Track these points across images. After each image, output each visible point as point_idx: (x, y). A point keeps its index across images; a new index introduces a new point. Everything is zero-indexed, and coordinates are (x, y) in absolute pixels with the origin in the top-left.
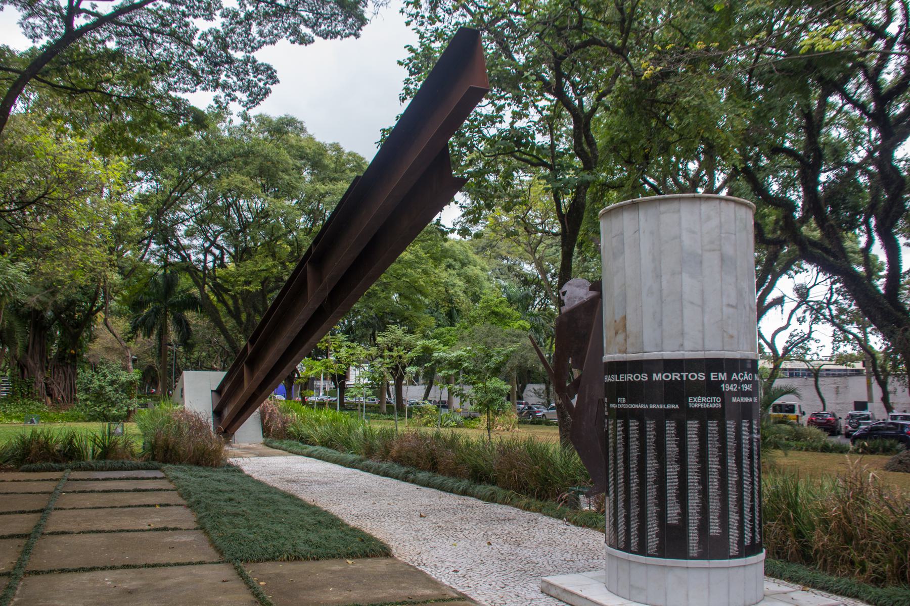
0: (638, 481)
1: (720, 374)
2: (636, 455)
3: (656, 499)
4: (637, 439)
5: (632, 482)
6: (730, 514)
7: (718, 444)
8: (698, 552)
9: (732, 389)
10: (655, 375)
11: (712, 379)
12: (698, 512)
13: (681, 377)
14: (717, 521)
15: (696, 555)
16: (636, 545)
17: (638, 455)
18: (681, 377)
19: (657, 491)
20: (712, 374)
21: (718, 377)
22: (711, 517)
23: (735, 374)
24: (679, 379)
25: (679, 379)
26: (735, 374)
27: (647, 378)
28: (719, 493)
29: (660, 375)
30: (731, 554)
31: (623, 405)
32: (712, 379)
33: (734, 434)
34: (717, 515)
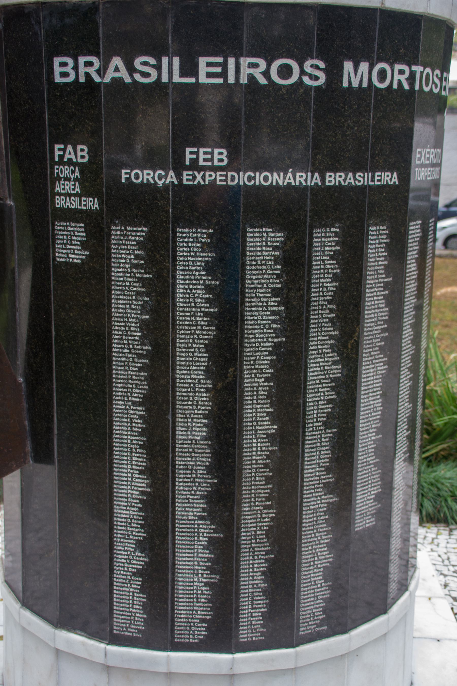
0: (272, 429)
2: (268, 346)
3: (328, 470)
4: (275, 292)
5: (248, 435)
10: (348, 66)
13: (412, 77)
16: (258, 621)
17: (277, 346)
18: (412, 77)
19: (333, 448)
24: (406, 87)
25: (406, 87)
27: (322, 78)
29: (364, 67)
31: (209, 176)
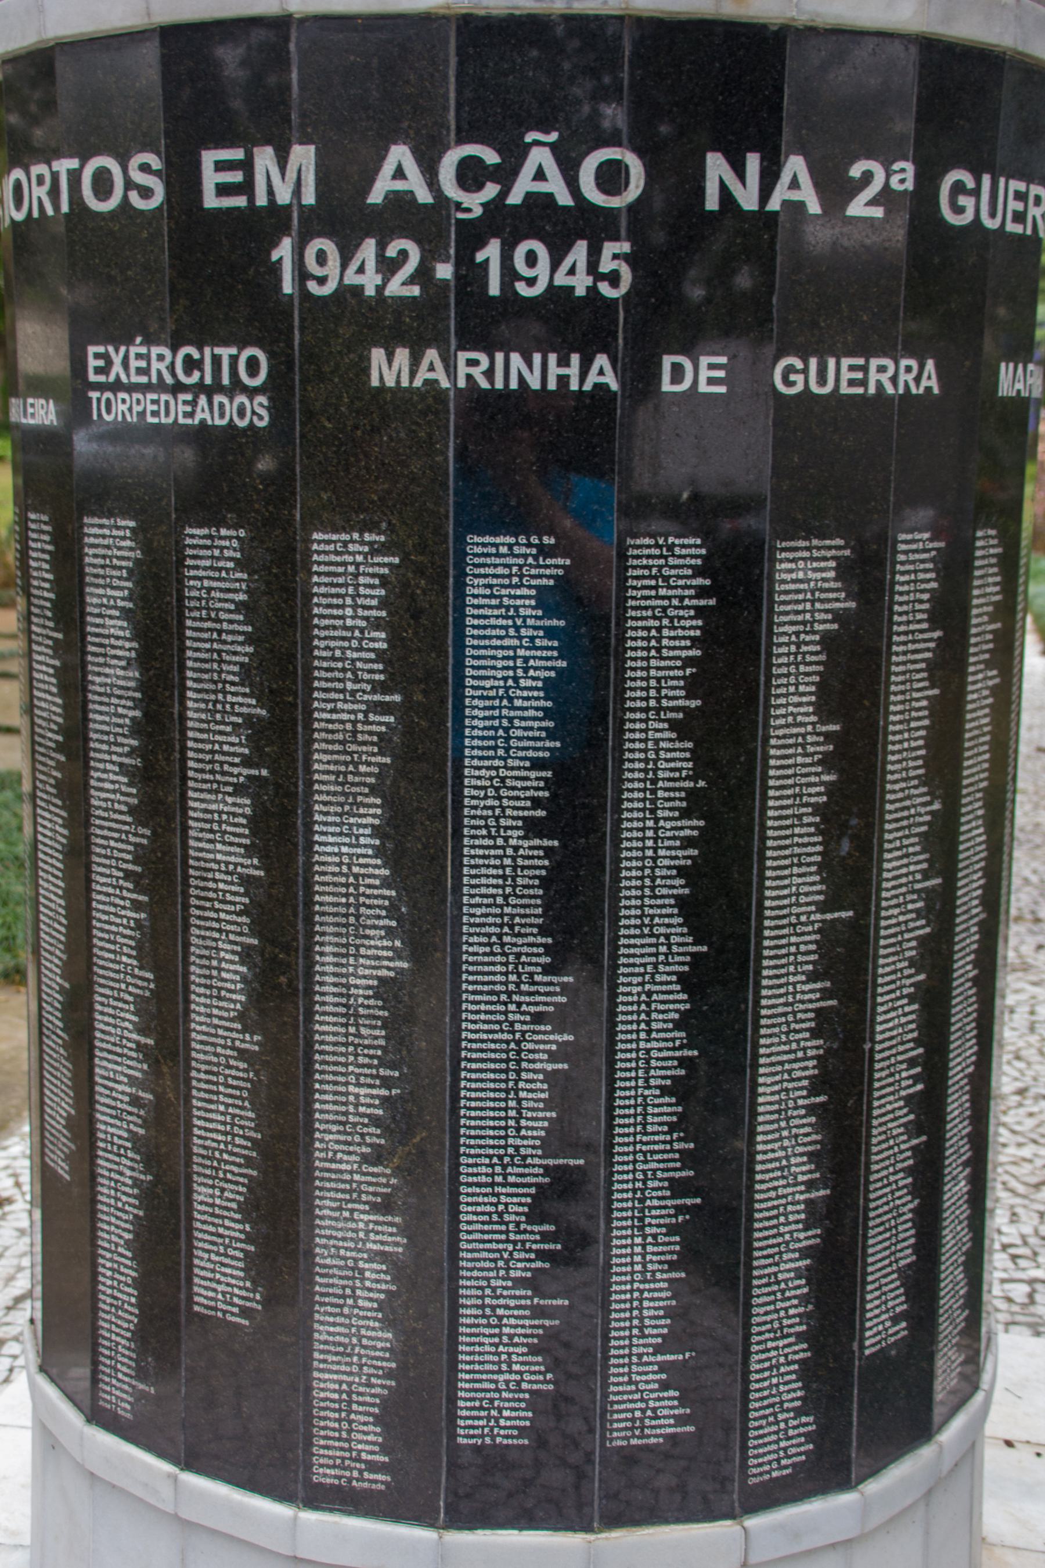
1: (265, 158)
6: (325, 1205)
7: (245, 704)
8: (140, 1396)
9: (370, 282)
11: (211, 201)
12: (133, 1137)
14: (235, 1228)
15: (125, 1410)
20: (209, 158)
21: (247, 188)
22: (202, 1193)
23: (400, 154)
26: (400, 154)
28: (251, 1042)
30: (324, 1474)
32: (211, 201)
33: (379, 641)
34: (235, 1194)
